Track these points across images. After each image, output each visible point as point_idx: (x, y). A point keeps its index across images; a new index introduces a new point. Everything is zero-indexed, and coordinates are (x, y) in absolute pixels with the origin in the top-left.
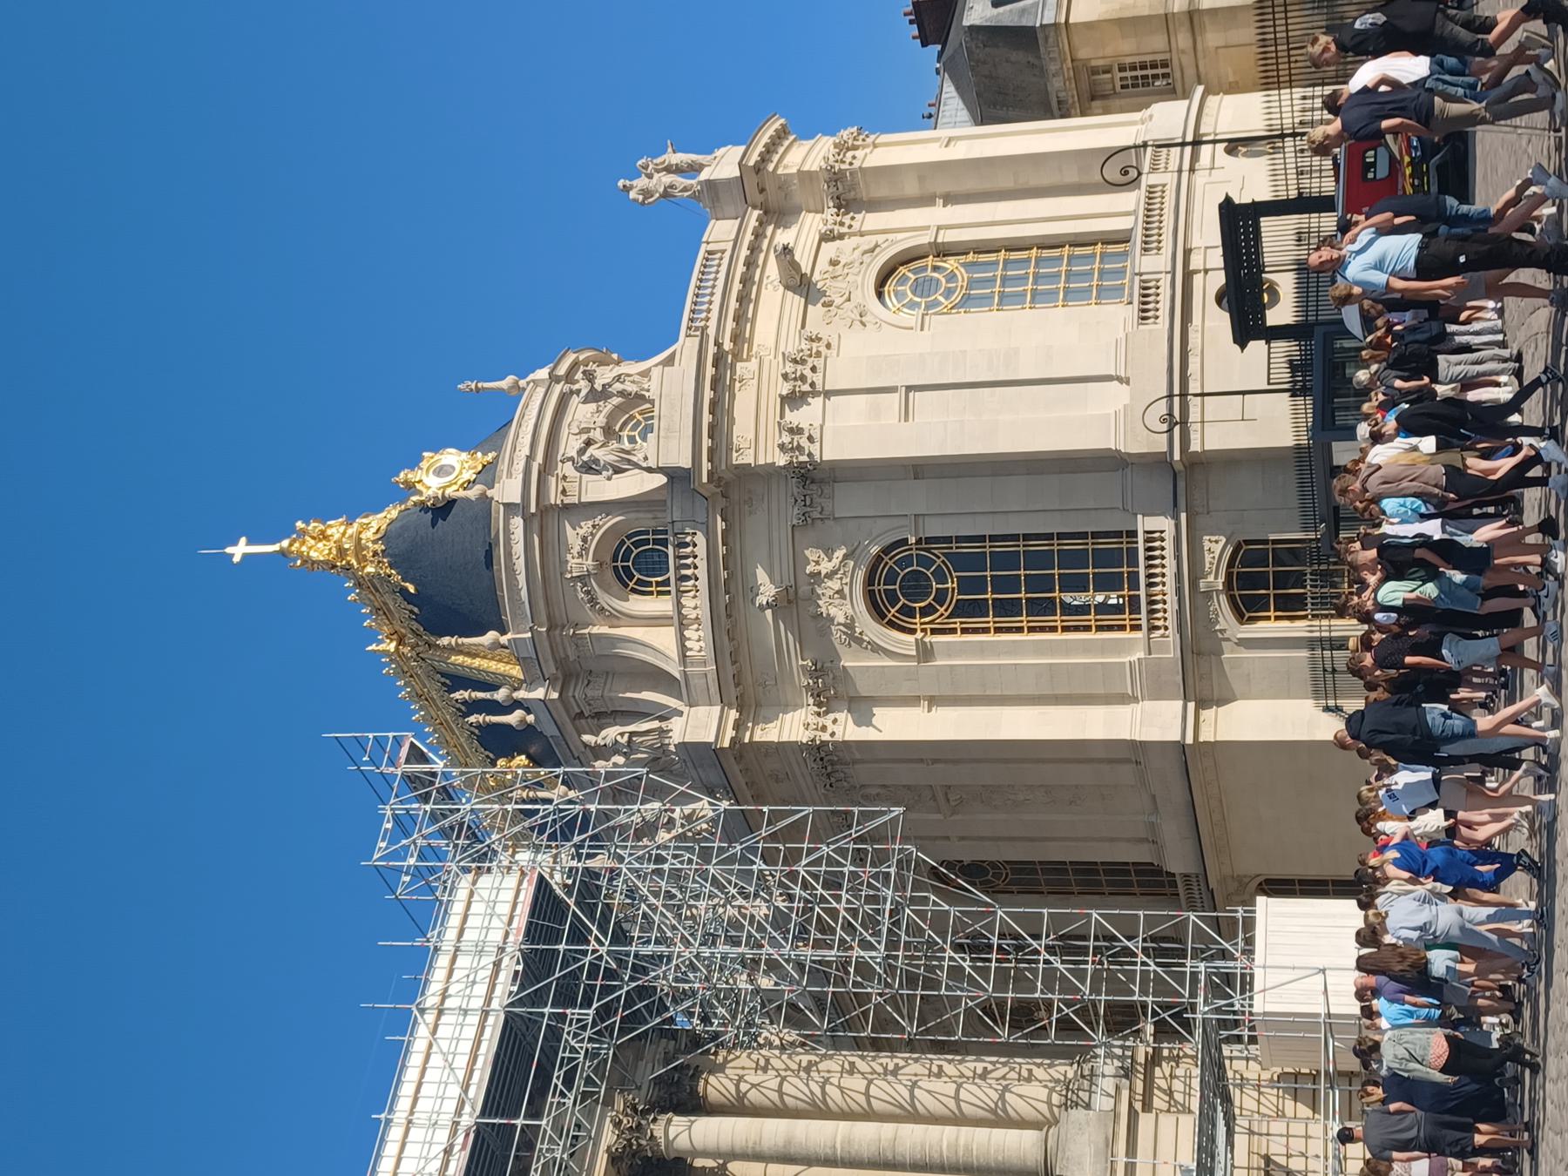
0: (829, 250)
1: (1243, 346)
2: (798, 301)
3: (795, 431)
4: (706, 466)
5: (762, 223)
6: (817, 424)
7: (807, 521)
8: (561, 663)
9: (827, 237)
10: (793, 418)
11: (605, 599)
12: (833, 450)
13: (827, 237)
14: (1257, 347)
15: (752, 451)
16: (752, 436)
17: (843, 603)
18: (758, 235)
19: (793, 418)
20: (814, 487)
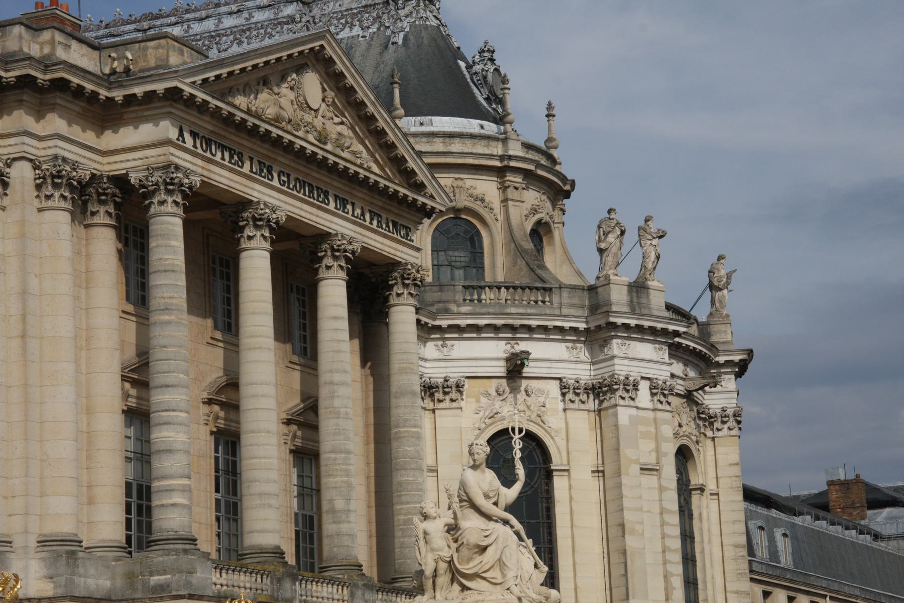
3: (636, 386)
4: (619, 321)
7: (564, 388)
10: (644, 386)
15: (621, 355)
16: (630, 355)
19: (644, 386)
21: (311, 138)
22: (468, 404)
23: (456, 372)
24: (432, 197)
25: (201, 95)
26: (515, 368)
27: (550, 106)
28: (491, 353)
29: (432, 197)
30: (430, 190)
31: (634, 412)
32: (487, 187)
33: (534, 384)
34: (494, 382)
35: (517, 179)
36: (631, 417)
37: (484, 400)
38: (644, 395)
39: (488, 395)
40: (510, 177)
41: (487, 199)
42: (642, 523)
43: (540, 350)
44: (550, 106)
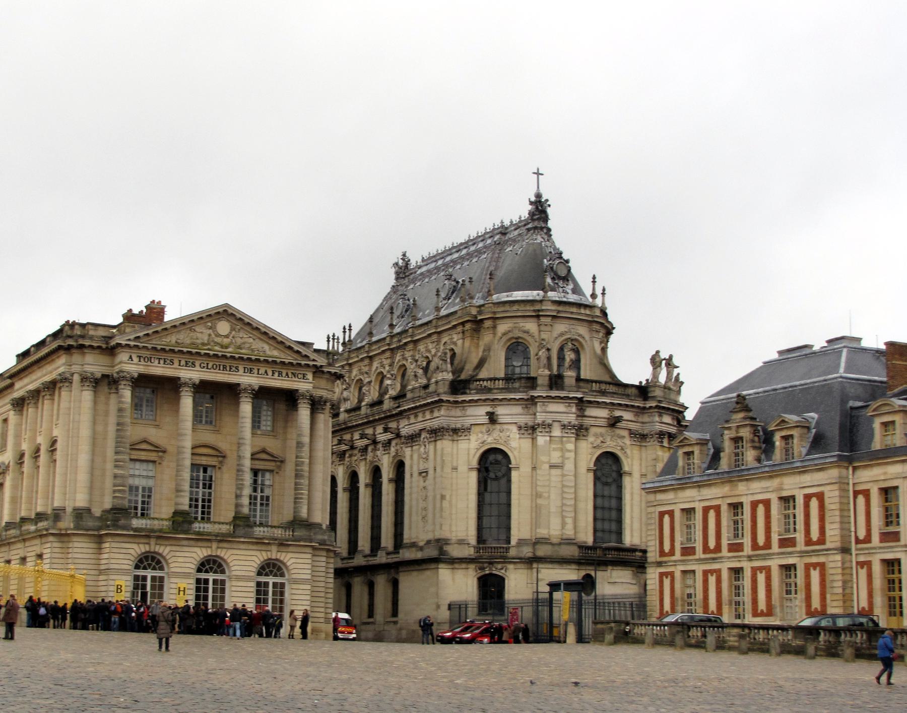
0: (625, 433)
1: (548, 585)
2: (603, 422)
3: (550, 426)
4: (536, 395)
5: (638, 407)
6: (553, 434)
7: (520, 428)
8: (482, 320)
9: (632, 433)
11: (505, 339)
12: (542, 440)
13: (632, 433)
14: (547, 589)
17: (491, 441)
18: (633, 406)
20: (530, 431)
21: (217, 348)
22: (473, 437)
23: (468, 422)
24: (314, 360)
25: (132, 343)
26: (492, 418)
27: (594, 277)
28: (479, 413)
29: (314, 360)
30: (312, 357)
31: (548, 438)
32: (531, 326)
33: (505, 427)
34: (485, 427)
35: (549, 320)
36: (545, 441)
37: (480, 435)
38: (557, 432)
39: (482, 432)
40: (543, 319)
41: (531, 331)
42: (549, 492)
43: (500, 411)
44: (594, 277)
